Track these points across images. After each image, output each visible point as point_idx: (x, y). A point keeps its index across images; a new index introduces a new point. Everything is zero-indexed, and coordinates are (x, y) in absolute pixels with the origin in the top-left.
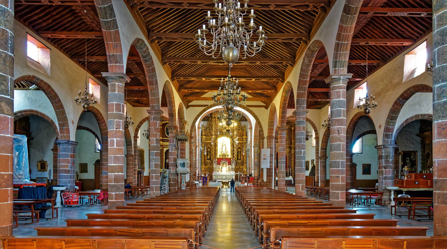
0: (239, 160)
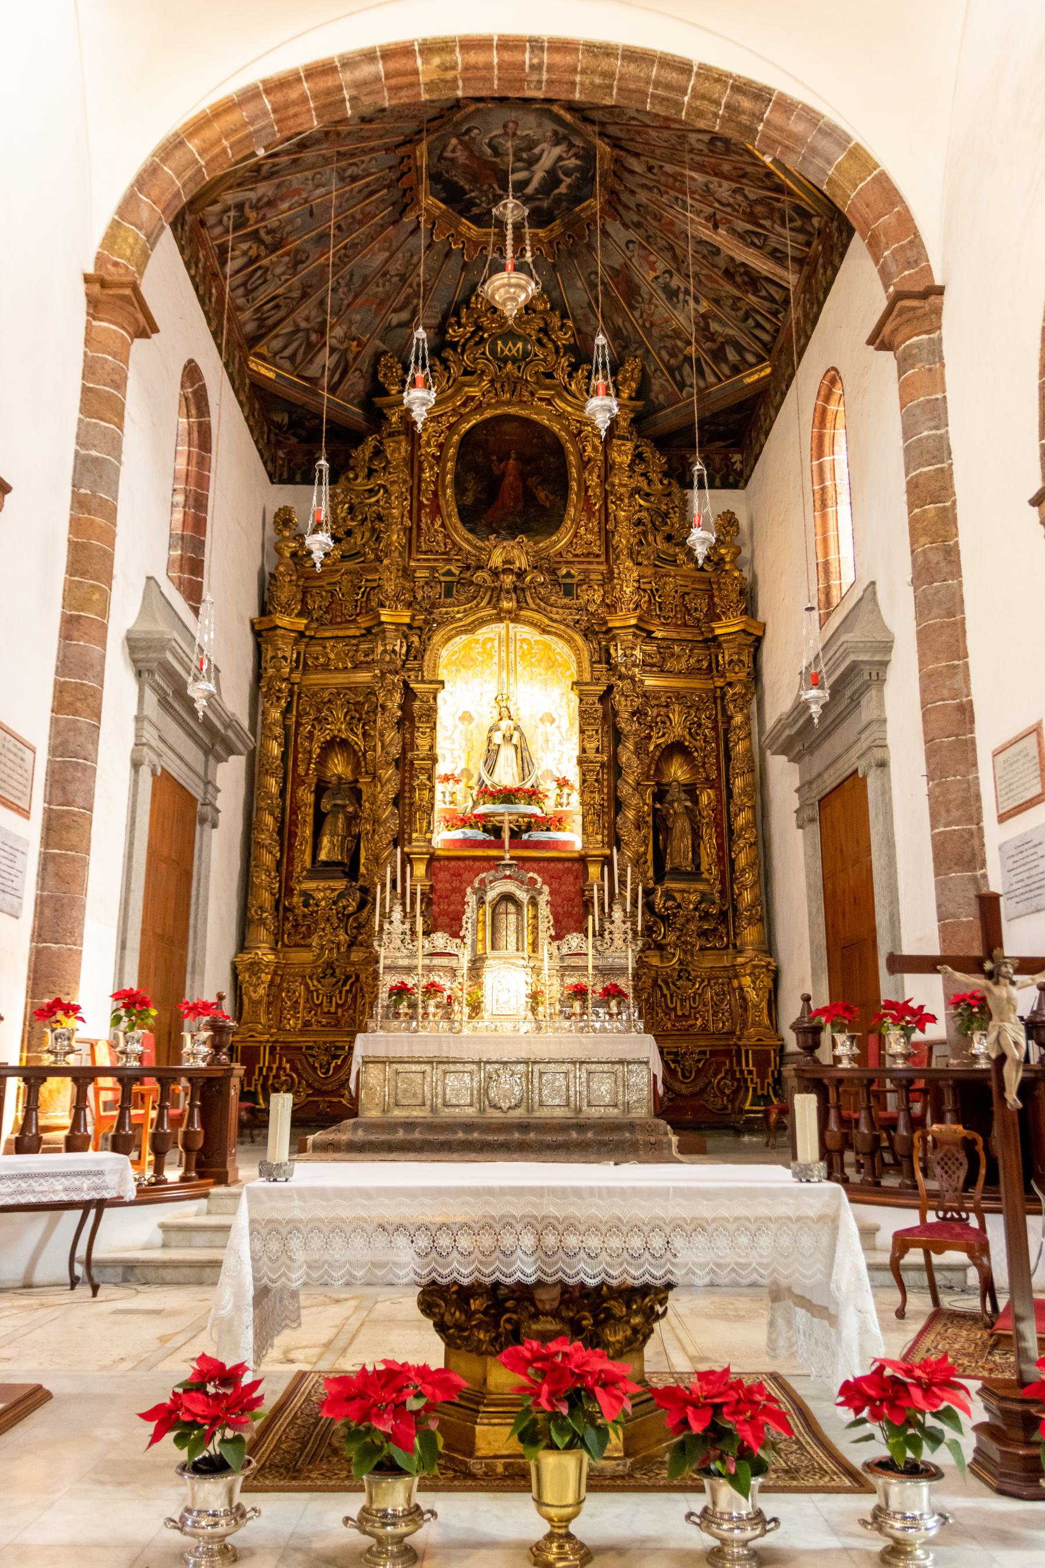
0: (678, 874)
